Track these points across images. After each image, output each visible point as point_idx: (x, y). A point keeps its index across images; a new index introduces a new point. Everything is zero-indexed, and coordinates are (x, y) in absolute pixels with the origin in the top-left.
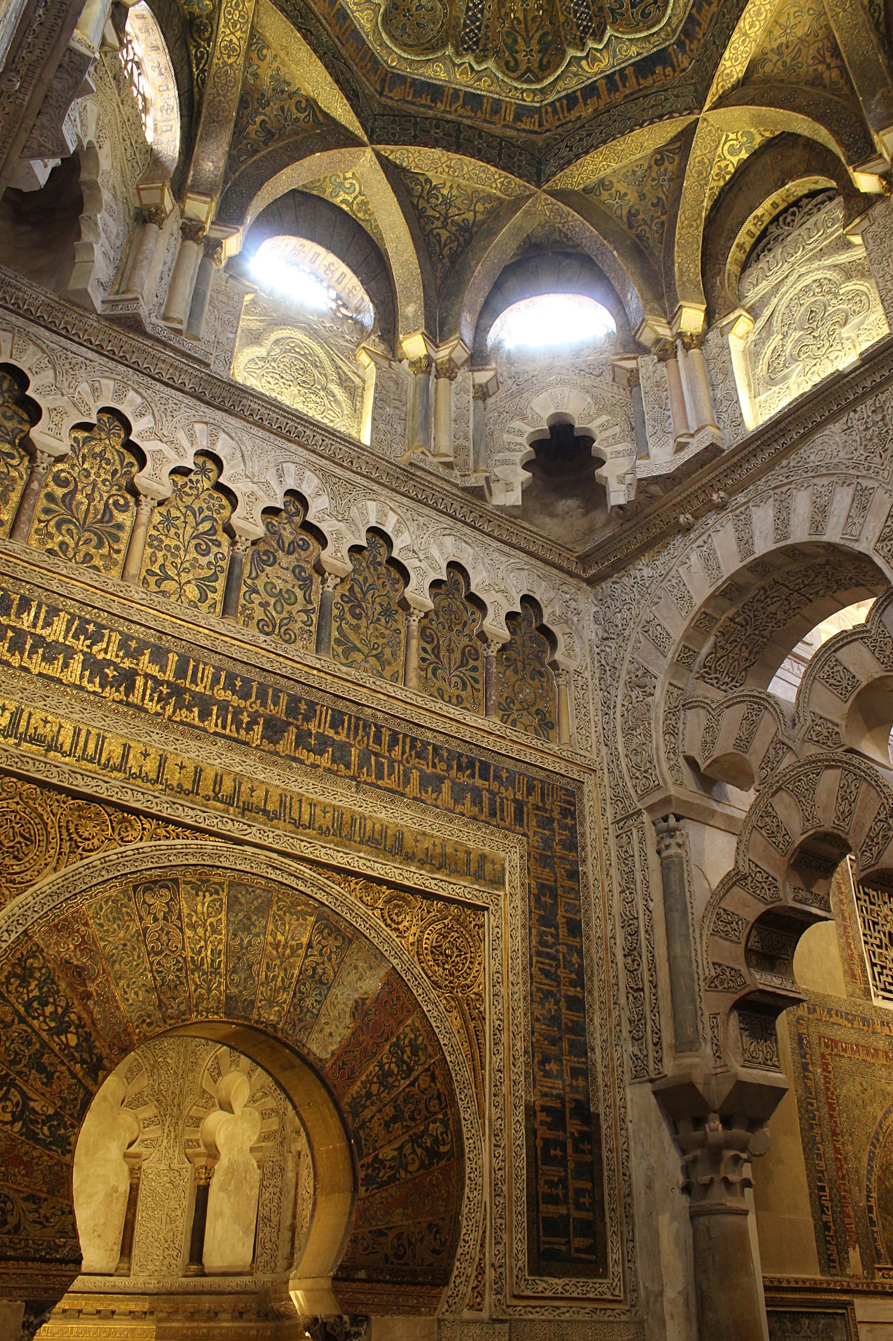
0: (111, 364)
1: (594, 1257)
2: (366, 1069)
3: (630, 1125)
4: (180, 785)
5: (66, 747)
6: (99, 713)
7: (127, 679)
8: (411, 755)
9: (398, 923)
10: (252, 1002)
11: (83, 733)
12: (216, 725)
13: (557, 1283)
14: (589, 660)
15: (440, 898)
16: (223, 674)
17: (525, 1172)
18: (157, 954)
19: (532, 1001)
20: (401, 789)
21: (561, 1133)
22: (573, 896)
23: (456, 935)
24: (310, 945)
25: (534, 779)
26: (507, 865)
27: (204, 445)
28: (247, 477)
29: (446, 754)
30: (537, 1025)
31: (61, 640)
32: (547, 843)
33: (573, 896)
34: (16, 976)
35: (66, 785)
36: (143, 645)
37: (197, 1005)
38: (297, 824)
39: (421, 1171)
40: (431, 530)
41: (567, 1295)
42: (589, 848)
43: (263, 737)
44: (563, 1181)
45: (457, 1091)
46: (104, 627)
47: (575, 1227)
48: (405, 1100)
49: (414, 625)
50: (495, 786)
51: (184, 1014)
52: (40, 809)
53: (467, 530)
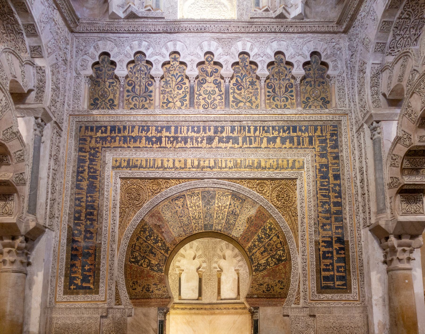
0: (135, 35)
1: (345, 287)
2: (253, 238)
3: (363, 243)
4: (180, 167)
5: (144, 166)
6: (152, 153)
7: (159, 140)
8: (263, 133)
9: (262, 191)
10: (212, 225)
11: (148, 161)
12: (190, 145)
13: (329, 296)
14: (345, 68)
15: (277, 179)
16: (190, 127)
17: (315, 263)
18: (182, 217)
19: (318, 206)
20: (260, 146)
21: (331, 249)
22: (336, 165)
23: (285, 190)
24: (230, 204)
25: (317, 126)
26: (305, 161)
27: (172, 49)
28: (189, 54)
29: (277, 128)
30: (320, 214)
31: (137, 135)
32: (324, 149)
33: (336, 165)
34: (142, 231)
35: (147, 177)
36: (162, 128)
37: (195, 229)
38: (221, 168)
39: (275, 266)
40: (265, 43)
41: (334, 299)
42: (344, 146)
43: (206, 144)
44: (332, 264)
45: (288, 240)
46: (150, 126)
47: (337, 279)
48: (268, 245)
49: (263, 83)
50: (299, 133)
51: (191, 232)
52: (141, 186)
53: (283, 35)
